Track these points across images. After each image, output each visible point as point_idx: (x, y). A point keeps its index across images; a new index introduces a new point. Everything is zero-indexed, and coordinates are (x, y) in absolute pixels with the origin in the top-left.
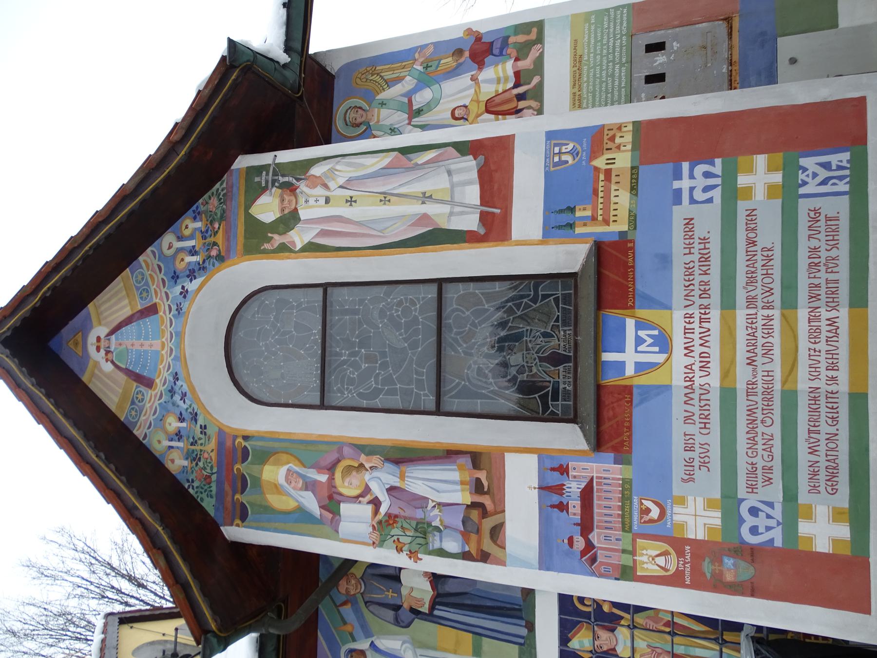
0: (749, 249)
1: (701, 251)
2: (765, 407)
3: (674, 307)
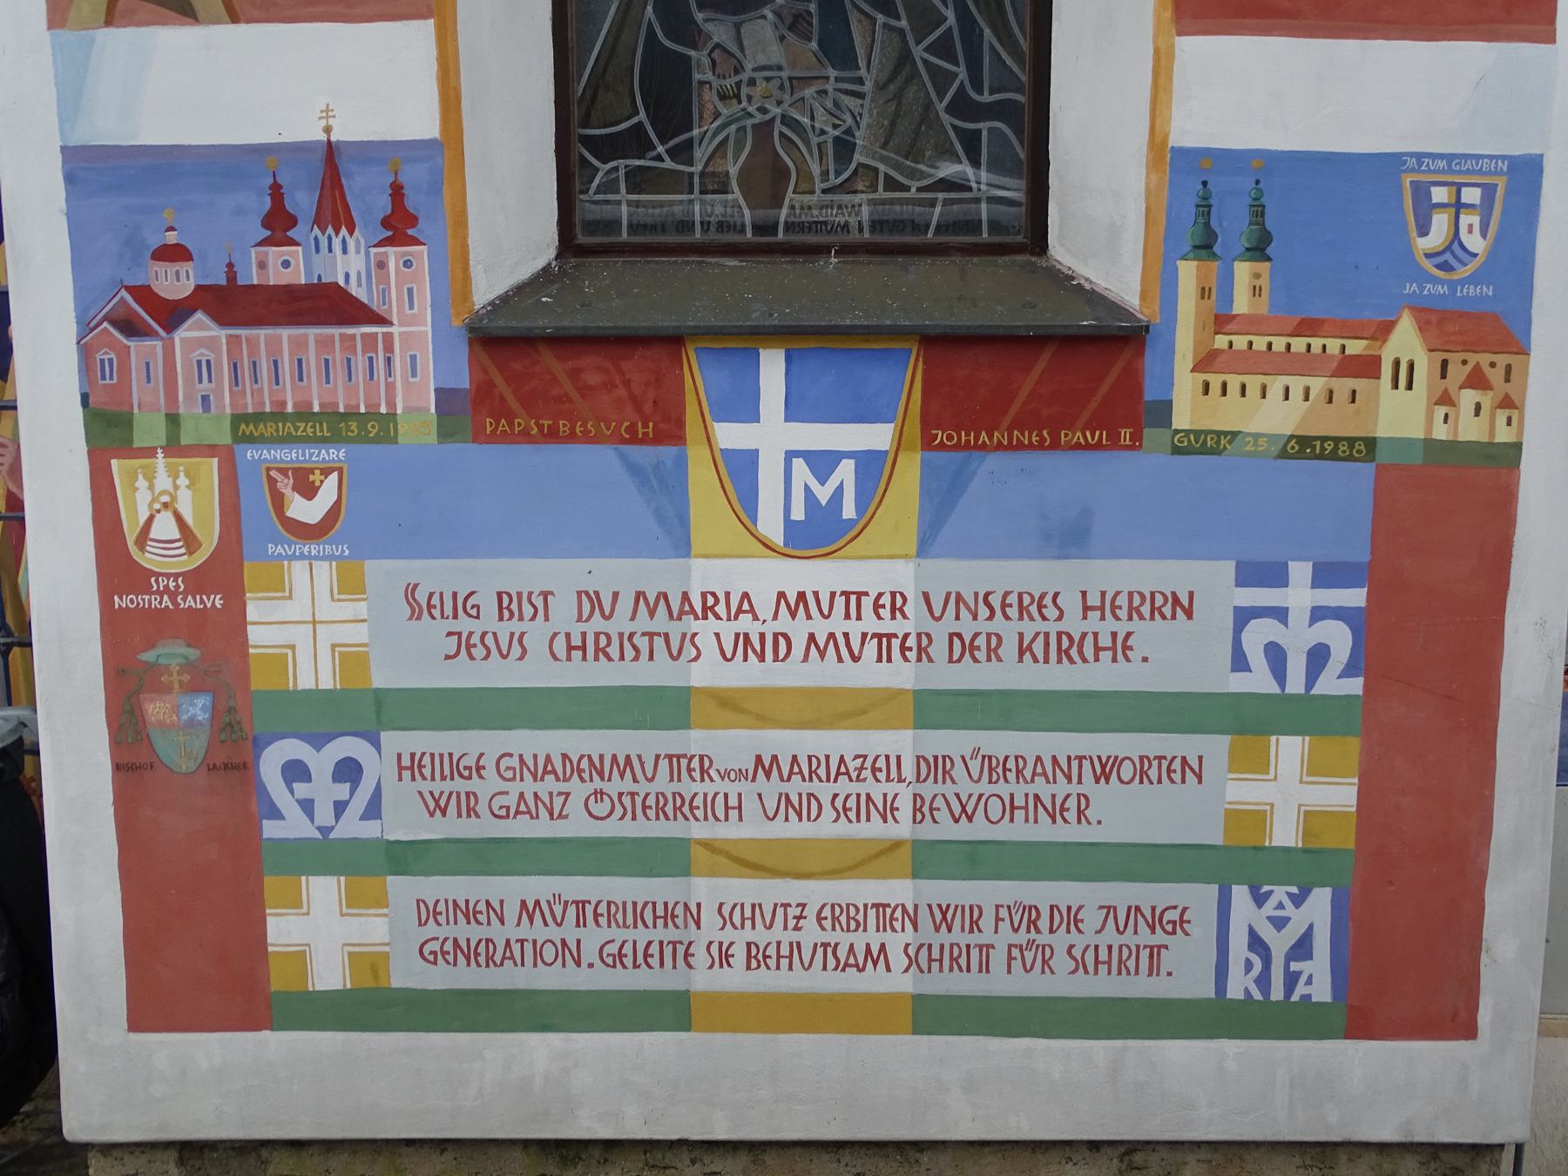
0: (1086, 763)
1: (1089, 640)
2: (639, 800)
3: (927, 563)
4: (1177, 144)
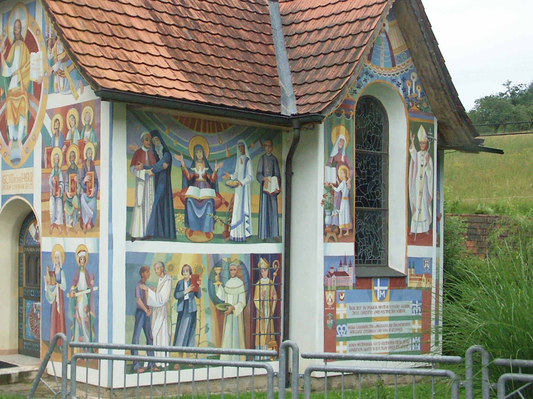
4: (409, 256)
